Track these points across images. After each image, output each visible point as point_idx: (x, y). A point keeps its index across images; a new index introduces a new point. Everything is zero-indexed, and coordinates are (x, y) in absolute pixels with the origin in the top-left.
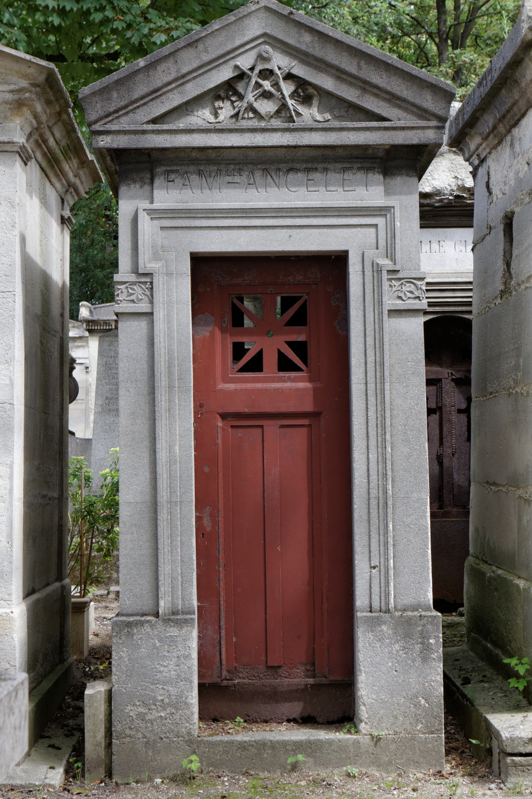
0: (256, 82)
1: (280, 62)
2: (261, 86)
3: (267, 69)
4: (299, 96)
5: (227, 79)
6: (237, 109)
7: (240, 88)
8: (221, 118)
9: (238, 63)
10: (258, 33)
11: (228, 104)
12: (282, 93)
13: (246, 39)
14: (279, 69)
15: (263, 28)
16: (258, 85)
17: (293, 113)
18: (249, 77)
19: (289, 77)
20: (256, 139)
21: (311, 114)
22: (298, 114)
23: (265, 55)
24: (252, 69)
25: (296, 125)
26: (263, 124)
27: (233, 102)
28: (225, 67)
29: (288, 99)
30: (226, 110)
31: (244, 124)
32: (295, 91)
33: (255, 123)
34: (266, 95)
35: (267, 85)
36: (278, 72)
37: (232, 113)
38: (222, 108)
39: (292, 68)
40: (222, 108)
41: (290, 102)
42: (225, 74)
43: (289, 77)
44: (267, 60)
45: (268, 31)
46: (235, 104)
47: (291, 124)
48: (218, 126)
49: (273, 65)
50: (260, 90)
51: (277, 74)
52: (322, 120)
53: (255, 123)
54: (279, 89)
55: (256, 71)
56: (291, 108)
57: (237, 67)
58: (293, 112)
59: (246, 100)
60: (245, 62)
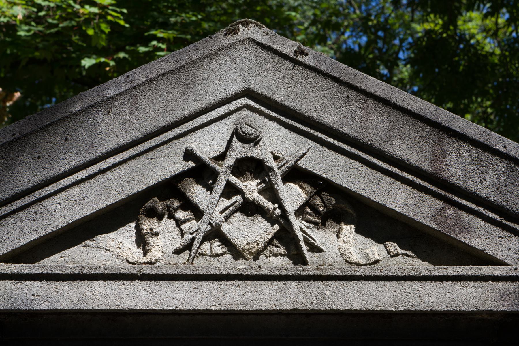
0: (229, 184)
1: (277, 143)
2: (239, 191)
3: (252, 159)
4: (316, 212)
5: (169, 176)
6: (188, 237)
7: (198, 193)
8: (155, 254)
9: (193, 146)
10: (236, 87)
11: (168, 224)
12: (281, 207)
13: (210, 100)
14: (276, 158)
15: (244, 79)
16: (231, 190)
17: (305, 248)
18: (214, 175)
19: (295, 174)
20: (227, 297)
21: (344, 244)
22: (315, 249)
23: (248, 130)
24: (221, 157)
25: (310, 270)
26: (240, 266)
27: (179, 223)
28: (166, 152)
29: (292, 218)
30: (166, 237)
31: (201, 265)
32: (308, 204)
33: (227, 263)
34: (250, 209)
35: (251, 187)
36: (274, 165)
37: (178, 243)
38: (157, 234)
39: (301, 157)
40: (157, 234)
41: (297, 223)
42: (169, 164)
43: (295, 174)
44: (255, 141)
45: (256, 87)
46: (184, 227)
47: (300, 267)
48: (148, 270)
49: (263, 152)
50: (238, 198)
51: (271, 169)
52: (363, 262)
53: (227, 263)
54: (275, 198)
55: (230, 161)
56: (300, 235)
57: (189, 155)
58: (302, 244)
59: (206, 218)
60: (209, 143)
